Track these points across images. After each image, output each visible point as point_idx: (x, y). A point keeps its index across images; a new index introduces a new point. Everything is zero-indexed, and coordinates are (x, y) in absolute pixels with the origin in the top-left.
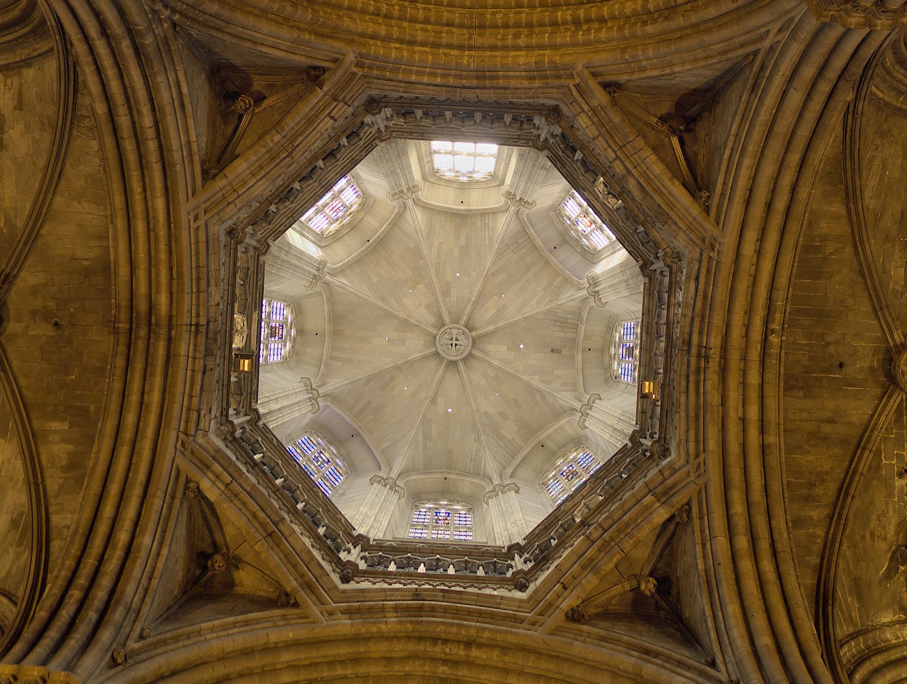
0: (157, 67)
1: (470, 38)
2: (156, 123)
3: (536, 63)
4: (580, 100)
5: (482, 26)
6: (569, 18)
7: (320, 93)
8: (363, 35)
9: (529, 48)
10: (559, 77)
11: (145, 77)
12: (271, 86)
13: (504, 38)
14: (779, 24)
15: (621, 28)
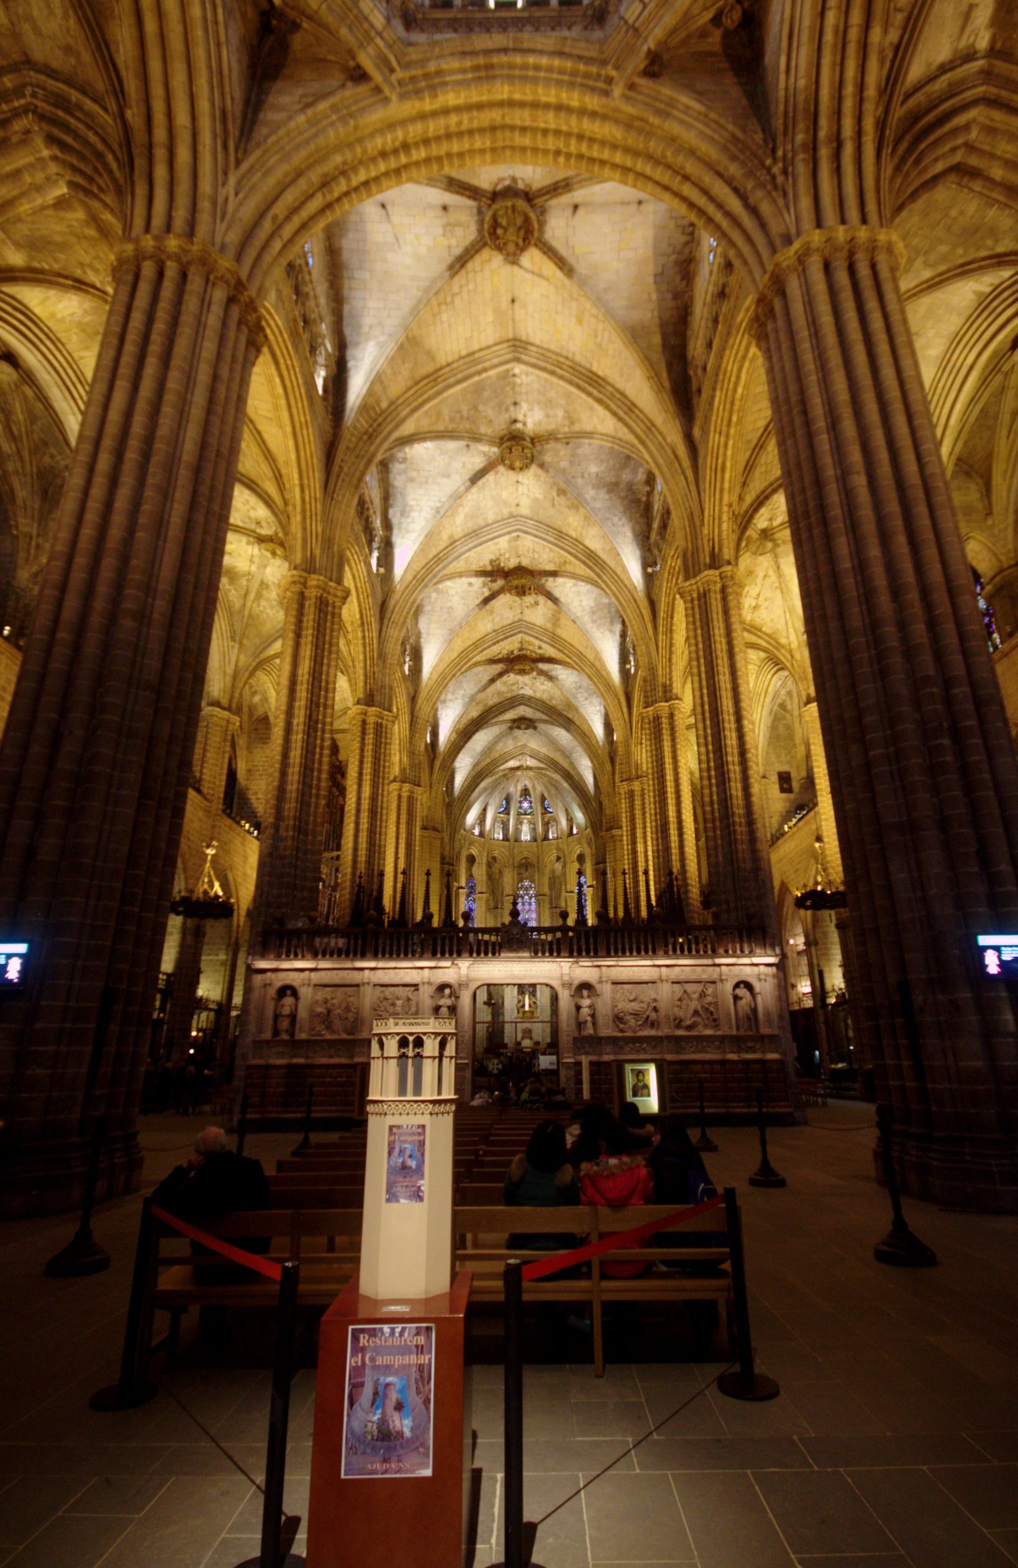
0: (801, 98)
1: (503, 117)
2: (822, 14)
3: (436, 96)
4: (386, 51)
5: (493, 129)
6: (414, 152)
7: (651, 44)
8: (605, 117)
9: (446, 111)
10: (413, 79)
11: (817, 82)
12: (703, 34)
13: (471, 120)
14: (231, 207)
15: (365, 151)
